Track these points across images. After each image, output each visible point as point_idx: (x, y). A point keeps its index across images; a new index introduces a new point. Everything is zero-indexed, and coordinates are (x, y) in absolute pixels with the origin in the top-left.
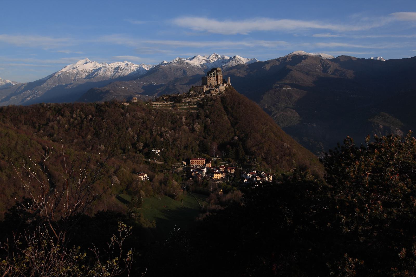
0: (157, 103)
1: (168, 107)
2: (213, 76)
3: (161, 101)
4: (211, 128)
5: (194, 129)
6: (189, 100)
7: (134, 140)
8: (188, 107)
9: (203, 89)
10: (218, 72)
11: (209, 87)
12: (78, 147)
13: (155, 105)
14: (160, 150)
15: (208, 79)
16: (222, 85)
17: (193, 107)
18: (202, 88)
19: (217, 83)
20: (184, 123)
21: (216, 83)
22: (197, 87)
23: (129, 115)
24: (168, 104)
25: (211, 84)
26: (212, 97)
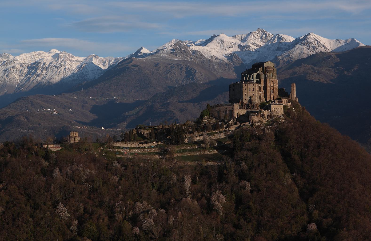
0: (126, 145)
1: (150, 154)
2: (255, 80)
3: (135, 140)
4: (251, 204)
5: (213, 205)
6: (201, 138)
7: (71, 231)
8: (198, 153)
9: (231, 112)
10: (267, 71)
11: (247, 106)
15: (244, 89)
16: (276, 102)
17: (210, 153)
18: (229, 108)
19: (266, 96)
20: (188, 192)
21: (263, 96)
23: (59, 174)
24: (150, 147)
26: (254, 130)
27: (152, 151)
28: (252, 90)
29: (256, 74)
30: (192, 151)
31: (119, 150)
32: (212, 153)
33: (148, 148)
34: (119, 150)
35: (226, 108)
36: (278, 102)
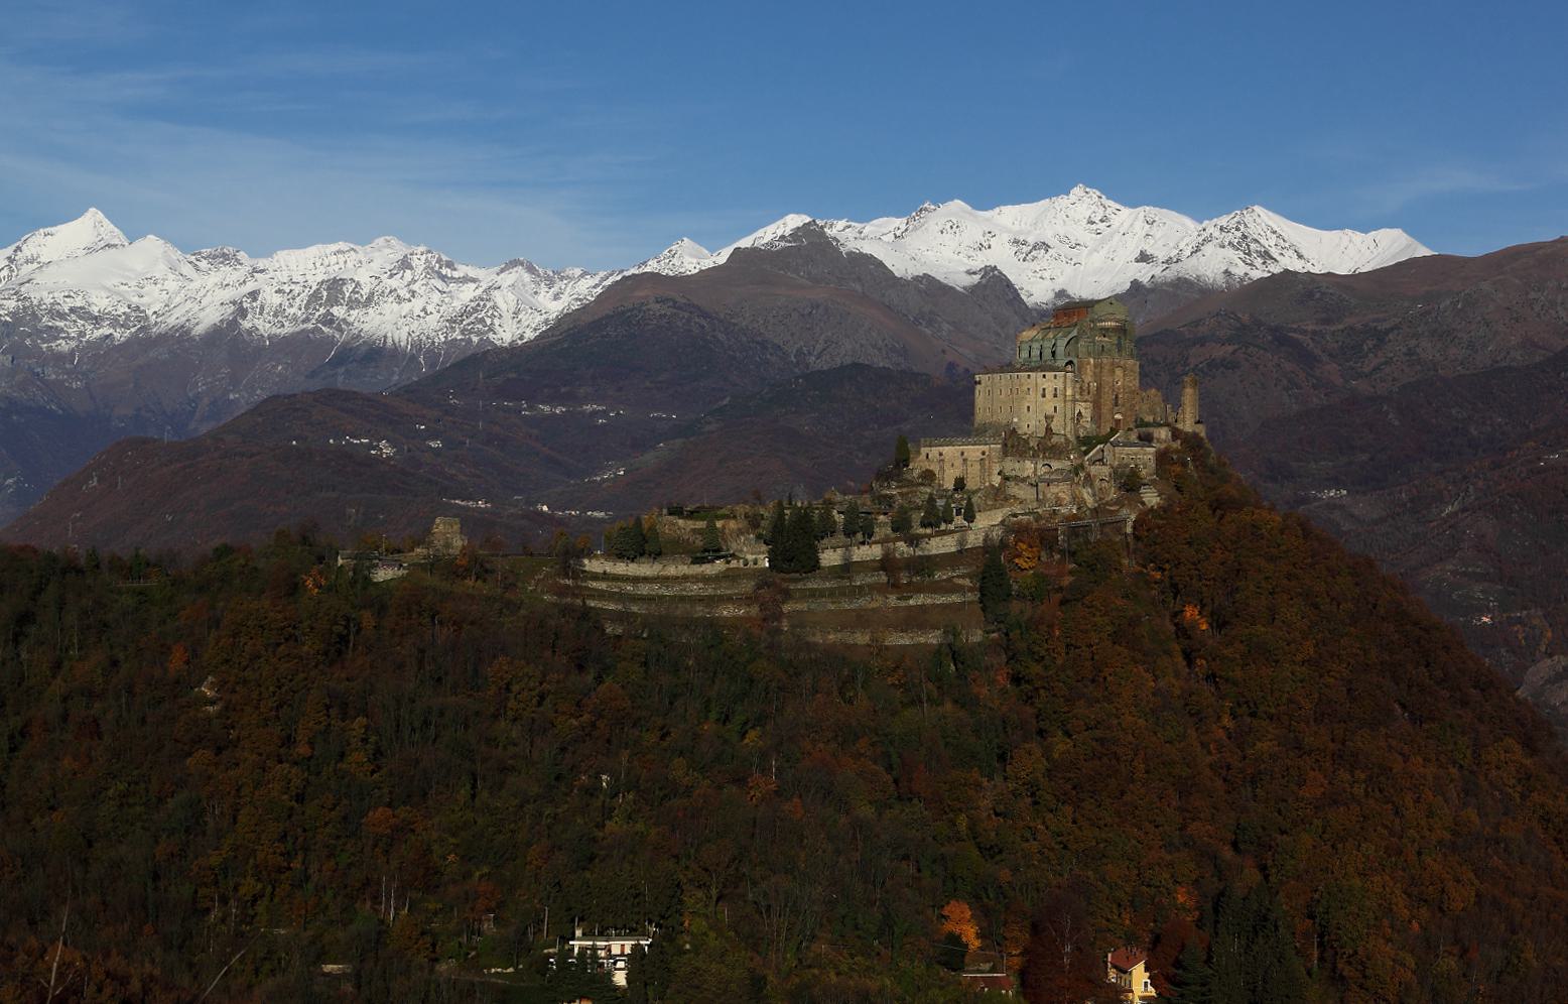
0: (620, 568)
1: (701, 600)
12: (725, 912)
13: (603, 586)
14: (628, 945)
16: (1133, 437)
17: (903, 604)
18: (974, 451)
21: (1087, 414)
22: (940, 446)
25: (1049, 430)
27: (710, 592)
28: (1049, 395)
29: (1067, 340)
30: (844, 595)
31: (594, 584)
32: (911, 602)
33: (696, 579)
34: (594, 584)
35: (962, 454)
36: (1140, 438)
